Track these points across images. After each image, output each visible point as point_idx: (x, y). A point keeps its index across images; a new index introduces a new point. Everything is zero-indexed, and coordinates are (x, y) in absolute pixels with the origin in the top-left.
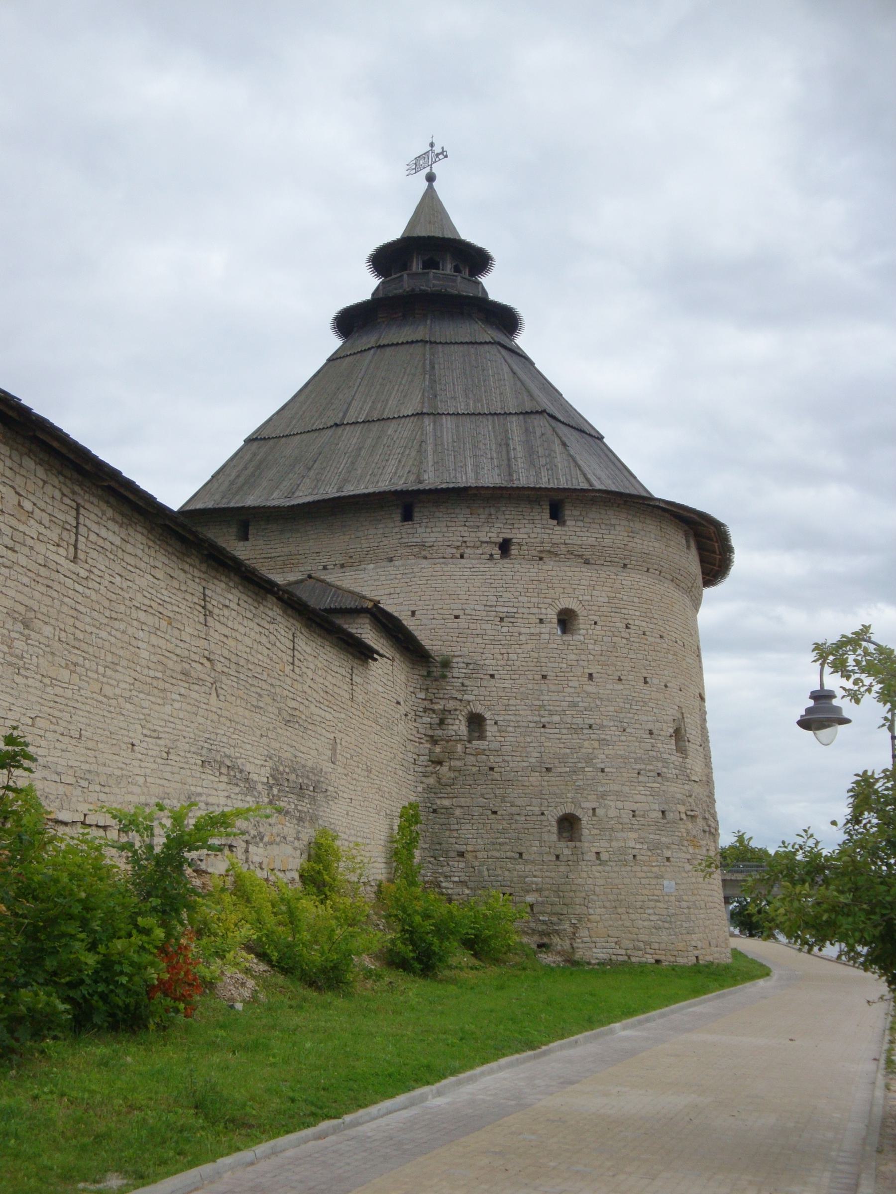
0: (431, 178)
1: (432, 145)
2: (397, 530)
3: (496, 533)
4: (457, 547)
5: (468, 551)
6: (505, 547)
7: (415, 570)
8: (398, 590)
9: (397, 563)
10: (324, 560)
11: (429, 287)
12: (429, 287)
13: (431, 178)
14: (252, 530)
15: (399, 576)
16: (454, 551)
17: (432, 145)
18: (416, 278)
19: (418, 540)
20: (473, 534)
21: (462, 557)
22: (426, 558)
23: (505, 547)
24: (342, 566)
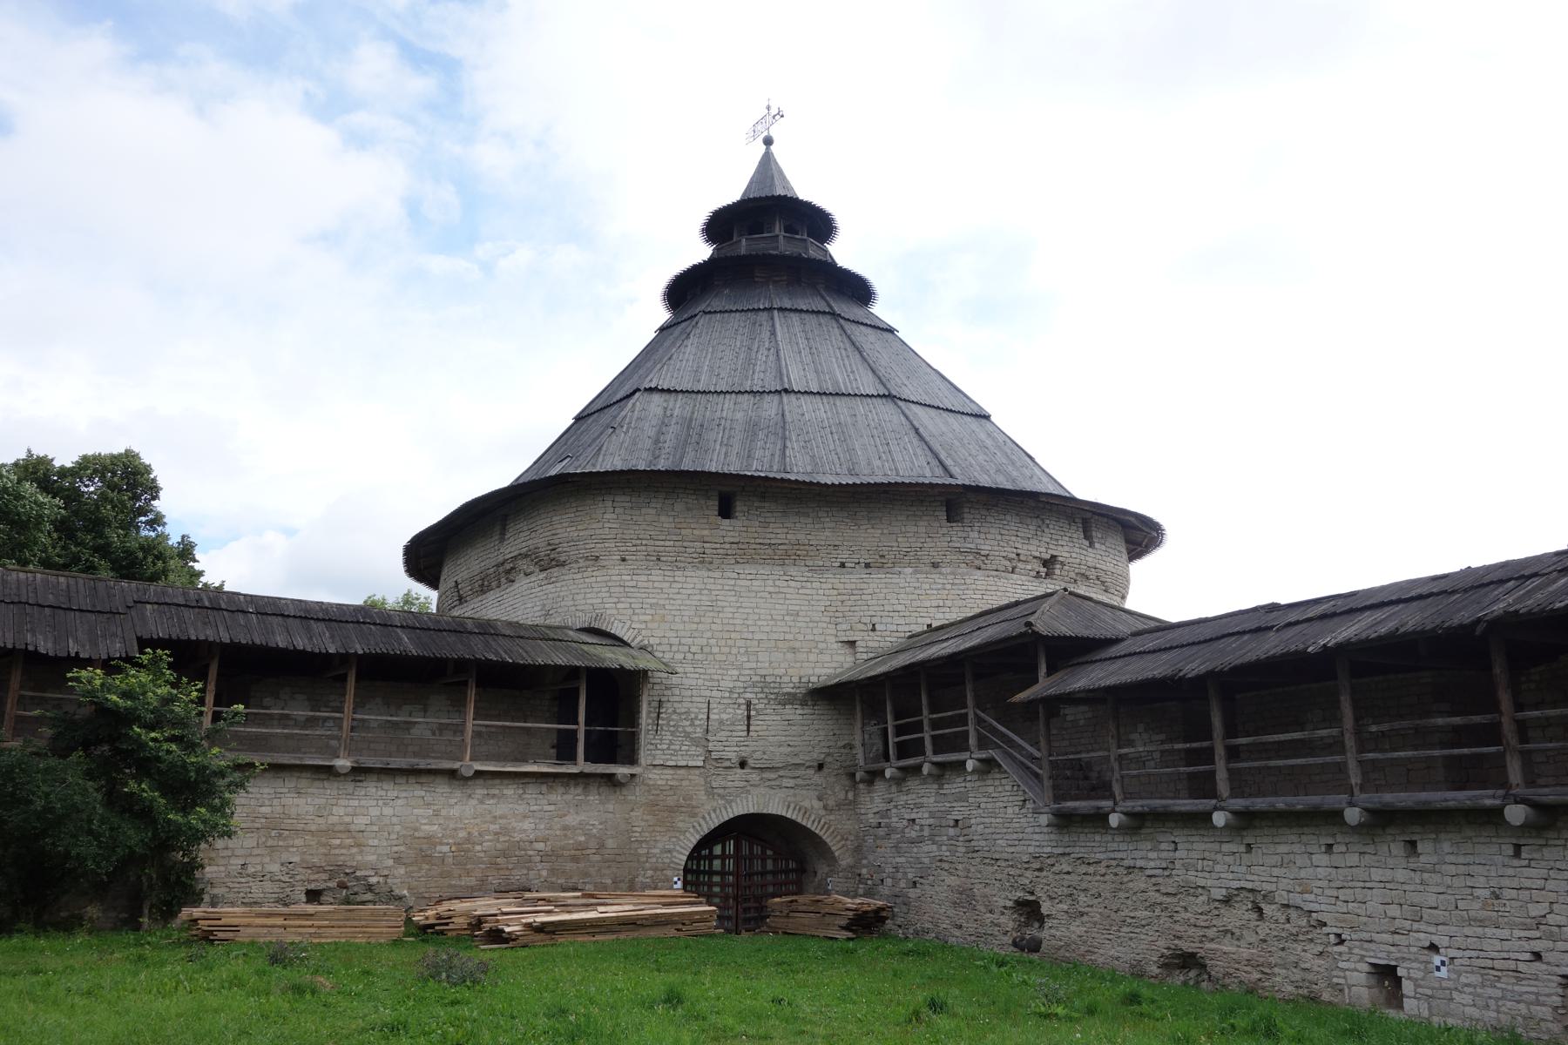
0: (768, 142)
1: (768, 108)
2: (945, 530)
3: (1039, 548)
4: (1010, 560)
5: (1020, 565)
8: (948, 603)
10: (844, 556)
11: (767, 253)
12: (767, 253)
13: (768, 142)
14: (739, 506)
17: (768, 108)
18: (781, 243)
24: (867, 566)
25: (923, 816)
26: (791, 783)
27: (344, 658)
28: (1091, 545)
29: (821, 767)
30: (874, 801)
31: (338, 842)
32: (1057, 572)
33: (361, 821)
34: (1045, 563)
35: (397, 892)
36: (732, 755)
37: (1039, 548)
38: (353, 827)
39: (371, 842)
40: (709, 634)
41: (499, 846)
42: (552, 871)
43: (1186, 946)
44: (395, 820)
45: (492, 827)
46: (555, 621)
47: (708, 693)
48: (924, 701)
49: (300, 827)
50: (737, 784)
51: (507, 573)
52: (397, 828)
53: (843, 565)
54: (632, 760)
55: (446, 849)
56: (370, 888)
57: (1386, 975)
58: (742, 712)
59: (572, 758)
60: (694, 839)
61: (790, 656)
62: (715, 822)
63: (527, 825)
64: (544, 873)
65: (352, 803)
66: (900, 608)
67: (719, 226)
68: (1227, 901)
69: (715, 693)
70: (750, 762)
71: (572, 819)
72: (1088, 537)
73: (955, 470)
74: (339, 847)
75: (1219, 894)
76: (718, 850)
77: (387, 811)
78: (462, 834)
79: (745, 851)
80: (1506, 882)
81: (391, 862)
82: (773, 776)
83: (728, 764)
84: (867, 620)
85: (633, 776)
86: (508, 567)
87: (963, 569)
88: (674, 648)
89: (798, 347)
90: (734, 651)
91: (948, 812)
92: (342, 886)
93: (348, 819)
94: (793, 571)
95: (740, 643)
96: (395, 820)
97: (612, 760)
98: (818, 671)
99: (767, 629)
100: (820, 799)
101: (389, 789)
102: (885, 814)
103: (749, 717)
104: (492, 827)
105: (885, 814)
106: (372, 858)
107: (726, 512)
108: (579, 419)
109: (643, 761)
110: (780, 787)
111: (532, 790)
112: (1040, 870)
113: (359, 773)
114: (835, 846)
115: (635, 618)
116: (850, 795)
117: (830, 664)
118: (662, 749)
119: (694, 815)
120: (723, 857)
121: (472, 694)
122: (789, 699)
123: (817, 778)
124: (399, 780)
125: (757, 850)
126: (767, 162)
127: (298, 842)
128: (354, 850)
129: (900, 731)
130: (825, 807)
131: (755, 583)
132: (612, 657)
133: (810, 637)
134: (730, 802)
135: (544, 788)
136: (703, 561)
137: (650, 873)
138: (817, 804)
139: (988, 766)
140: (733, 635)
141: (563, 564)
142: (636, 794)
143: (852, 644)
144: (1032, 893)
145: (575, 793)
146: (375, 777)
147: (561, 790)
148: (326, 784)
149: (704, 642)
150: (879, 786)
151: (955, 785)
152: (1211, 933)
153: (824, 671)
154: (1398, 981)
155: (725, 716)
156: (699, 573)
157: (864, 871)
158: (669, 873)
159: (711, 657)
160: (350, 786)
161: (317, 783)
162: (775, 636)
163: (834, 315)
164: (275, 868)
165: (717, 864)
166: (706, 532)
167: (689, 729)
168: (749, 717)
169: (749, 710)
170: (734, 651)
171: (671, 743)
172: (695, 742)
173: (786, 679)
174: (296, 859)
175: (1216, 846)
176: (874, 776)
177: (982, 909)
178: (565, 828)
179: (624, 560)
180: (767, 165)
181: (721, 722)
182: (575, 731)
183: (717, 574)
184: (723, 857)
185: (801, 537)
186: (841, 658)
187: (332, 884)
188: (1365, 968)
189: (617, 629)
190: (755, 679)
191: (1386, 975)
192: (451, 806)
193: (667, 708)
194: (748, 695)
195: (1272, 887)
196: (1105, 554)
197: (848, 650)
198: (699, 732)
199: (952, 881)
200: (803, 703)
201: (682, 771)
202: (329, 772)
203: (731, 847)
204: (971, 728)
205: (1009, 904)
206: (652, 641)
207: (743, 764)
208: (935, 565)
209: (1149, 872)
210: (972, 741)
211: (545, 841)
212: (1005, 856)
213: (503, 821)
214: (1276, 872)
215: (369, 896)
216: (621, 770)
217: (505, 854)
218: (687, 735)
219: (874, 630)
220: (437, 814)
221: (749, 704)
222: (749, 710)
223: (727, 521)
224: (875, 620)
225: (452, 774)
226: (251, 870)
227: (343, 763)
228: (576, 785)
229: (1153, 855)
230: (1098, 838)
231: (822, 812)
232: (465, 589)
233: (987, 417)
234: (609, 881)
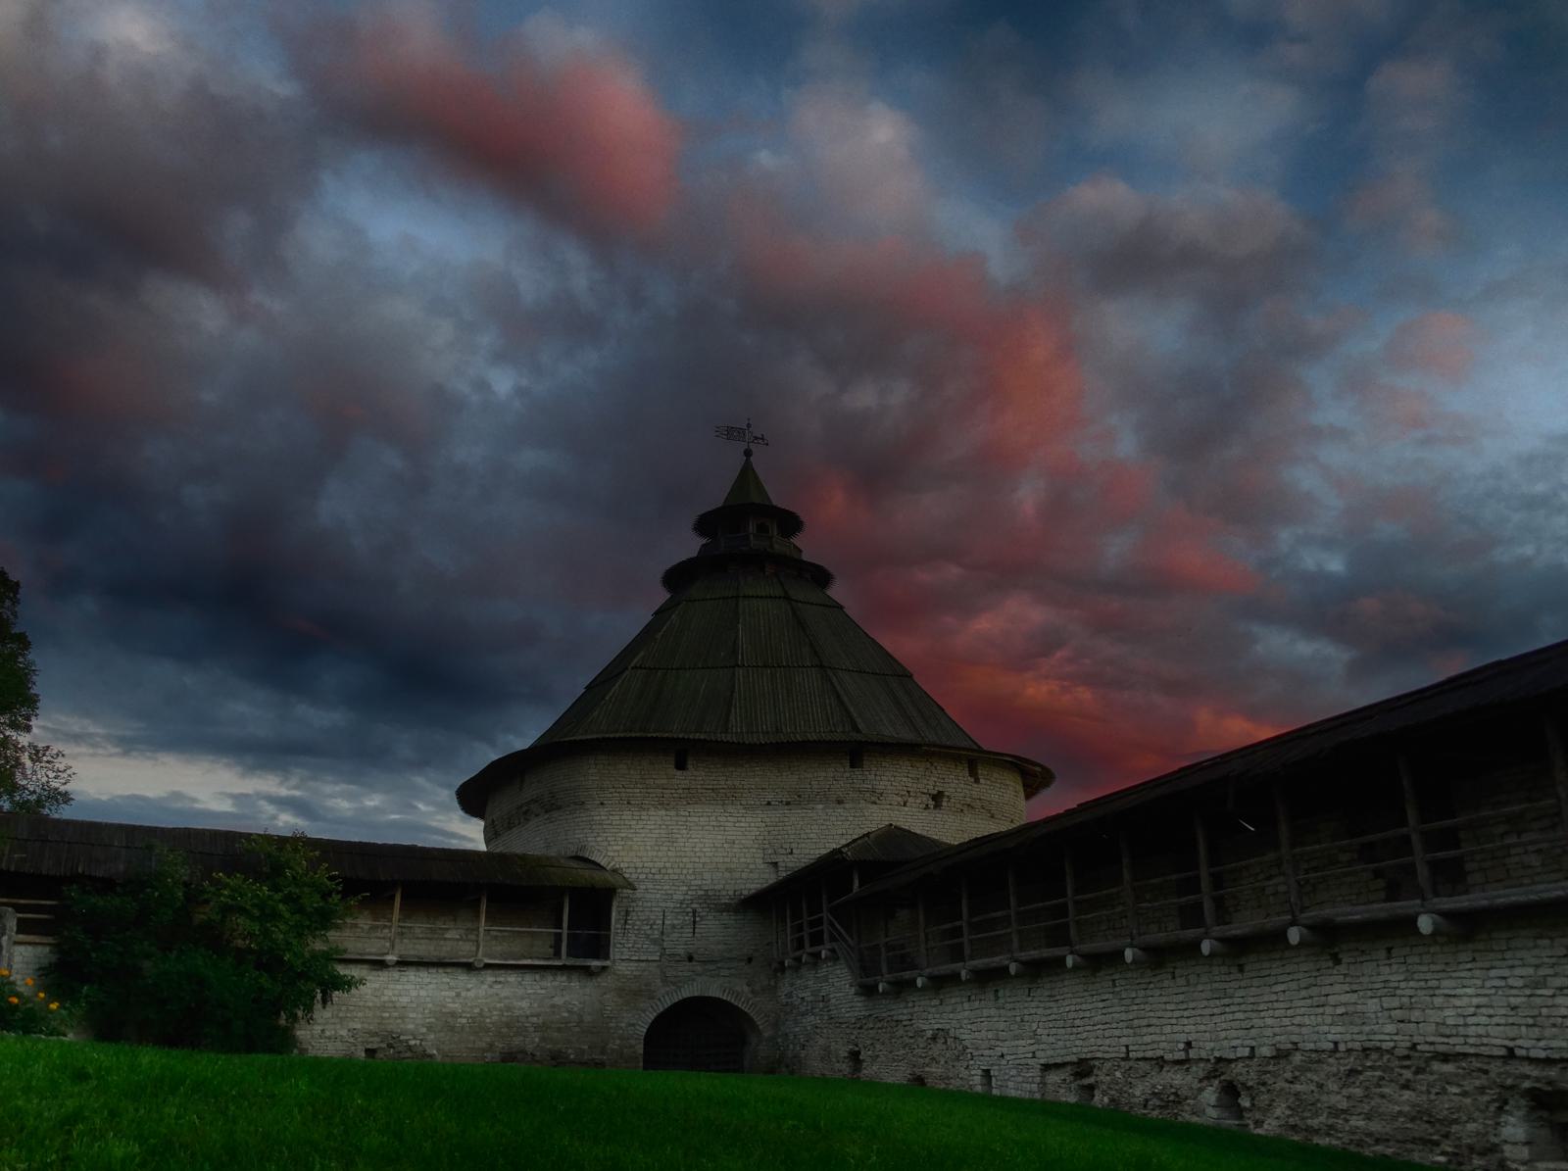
0: (748, 453)
2: (848, 775)
3: (931, 784)
5: (910, 800)
6: (937, 798)
7: (866, 814)
9: (847, 806)
10: (770, 797)
13: (748, 453)
15: (851, 819)
16: (900, 799)
19: (870, 786)
20: (915, 785)
21: (905, 805)
22: (876, 803)
23: (937, 798)
24: (788, 803)
25: (807, 994)
26: (726, 972)
28: (977, 781)
29: (750, 960)
31: (387, 1015)
32: (944, 804)
33: (404, 1000)
35: (429, 1051)
36: (681, 950)
37: (931, 784)
38: (398, 1005)
39: (411, 1015)
40: (666, 859)
41: (504, 1019)
42: (543, 1039)
43: (918, 1071)
44: (428, 999)
45: (498, 1005)
46: (552, 853)
47: (663, 904)
48: (804, 906)
49: (361, 1004)
50: (686, 974)
51: (524, 814)
52: (430, 1005)
53: (769, 803)
54: (607, 957)
55: (464, 1021)
56: (410, 1048)
57: (987, 1074)
58: (689, 918)
59: (557, 954)
61: (727, 875)
63: (524, 1004)
64: (537, 1040)
65: (398, 987)
66: (812, 836)
67: (705, 525)
68: (934, 1038)
69: (668, 904)
70: (695, 956)
71: (558, 1001)
72: (973, 773)
73: (861, 726)
74: (389, 1018)
75: (929, 1034)
77: (423, 993)
78: (477, 1011)
80: (1026, 1012)
81: (424, 1030)
82: (714, 967)
83: (678, 958)
84: (787, 846)
85: (604, 968)
86: (525, 809)
87: (863, 804)
88: (639, 871)
90: (685, 871)
91: (819, 991)
92: (390, 1046)
93: (394, 999)
94: (730, 809)
95: (690, 866)
96: (428, 999)
97: (597, 957)
98: (748, 886)
99: (711, 854)
100: (748, 985)
101: (424, 976)
102: (789, 995)
103: (694, 922)
104: (498, 1005)
105: (789, 995)
106: (411, 1026)
107: (681, 766)
108: (589, 688)
109: (611, 956)
110: (718, 975)
111: (528, 978)
112: (860, 1028)
113: (403, 964)
114: (759, 1021)
115: (610, 848)
116: (772, 983)
117: (758, 878)
119: (653, 998)
121: (483, 907)
122: (727, 908)
124: (433, 970)
126: (747, 474)
127: (360, 1014)
128: (399, 1021)
130: (753, 992)
131: (701, 819)
132: (586, 875)
133: (742, 860)
134: (679, 988)
135: (537, 977)
136: (663, 804)
137: (618, 1042)
138: (746, 989)
139: (834, 957)
140: (684, 860)
141: (559, 808)
142: (606, 981)
143: (775, 864)
144: (857, 1046)
145: (561, 979)
146: (414, 969)
147: (550, 978)
148: (380, 973)
149: (661, 865)
150: (788, 973)
151: (823, 971)
152: (927, 1060)
153: (752, 886)
154: (990, 1077)
155: (675, 922)
156: (660, 813)
157: (779, 1040)
158: (633, 1042)
159: (666, 877)
160: (396, 974)
161: (374, 973)
162: (717, 860)
163: (787, 598)
164: (344, 1033)
166: (665, 781)
167: (649, 932)
168: (694, 922)
169: (694, 916)
170: (685, 871)
171: (635, 943)
172: (654, 942)
173: (724, 893)
174: (358, 1026)
175: (928, 1002)
176: (782, 968)
177: (834, 1060)
178: (553, 1006)
179: (602, 804)
180: (747, 474)
181: (674, 926)
182: (560, 934)
183: (673, 813)
185: (737, 783)
186: (766, 876)
187: (384, 1045)
188: (979, 1072)
189: (598, 860)
190: (700, 893)
191: (987, 1074)
192: (468, 990)
193: (633, 916)
194: (694, 906)
195: (948, 1027)
197: (772, 870)
198: (656, 935)
199: (821, 1041)
201: (643, 964)
202: (380, 965)
204: (825, 927)
205: (846, 1055)
206: (622, 866)
207: (690, 959)
208: (840, 802)
209: (905, 1023)
210: (826, 936)
211: (537, 1015)
212: (845, 1020)
213: (507, 1001)
214: (951, 1016)
215: (409, 1054)
216: (595, 963)
217: (508, 1025)
218: (648, 936)
219: (791, 853)
220: (458, 995)
221: (694, 912)
222: (694, 916)
223: (679, 773)
224: (793, 846)
225: (469, 967)
226: (328, 1033)
227: (391, 958)
228: (562, 975)
229: (905, 1011)
230: (884, 1002)
231: (750, 996)
233: (911, 676)
234: (586, 1047)
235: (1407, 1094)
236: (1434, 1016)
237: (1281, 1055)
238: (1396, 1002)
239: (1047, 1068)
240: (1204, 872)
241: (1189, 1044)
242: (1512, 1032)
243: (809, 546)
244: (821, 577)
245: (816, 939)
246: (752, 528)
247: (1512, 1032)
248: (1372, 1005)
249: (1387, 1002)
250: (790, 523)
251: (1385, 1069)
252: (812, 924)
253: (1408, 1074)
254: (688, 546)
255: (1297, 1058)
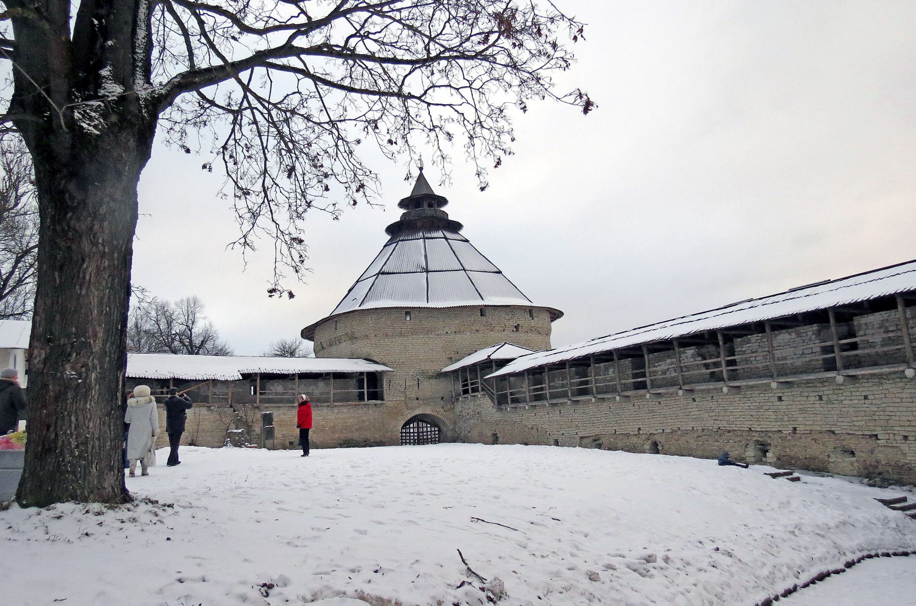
18: (427, 211)
27: (293, 375)
30: (458, 407)
34: (516, 327)
36: (414, 396)
60: (403, 423)
62: (409, 417)
67: (403, 204)
68: (532, 428)
72: (531, 315)
76: (412, 425)
79: (420, 425)
89: (436, 247)
118: (391, 396)
120: (413, 428)
123: (442, 402)
125: (425, 425)
129: (464, 386)
136: (401, 335)
165: (412, 430)
172: (402, 392)
184: (413, 428)
189: (375, 359)
196: (541, 320)
200: (436, 378)
203: (415, 424)
216: (379, 402)
232: (324, 345)
235: (716, 443)
236: (727, 418)
237: (673, 432)
238: (714, 414)
239: (582, 438)
240: (647, 370)
241: (640, 429)
242: (751, 423)
243: (452, 212)
244: (455, 227)
245: (475, 390)
246: (425, 204)
247: (751, 423)
248: (706, 415)
249: (711, 414)
250: (443, 201)
251: (710, 435)
252: (472, 384)
253: (717, 437)
254: (396, 215)
255: (679, 433)
